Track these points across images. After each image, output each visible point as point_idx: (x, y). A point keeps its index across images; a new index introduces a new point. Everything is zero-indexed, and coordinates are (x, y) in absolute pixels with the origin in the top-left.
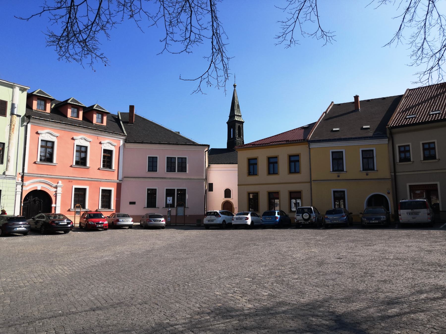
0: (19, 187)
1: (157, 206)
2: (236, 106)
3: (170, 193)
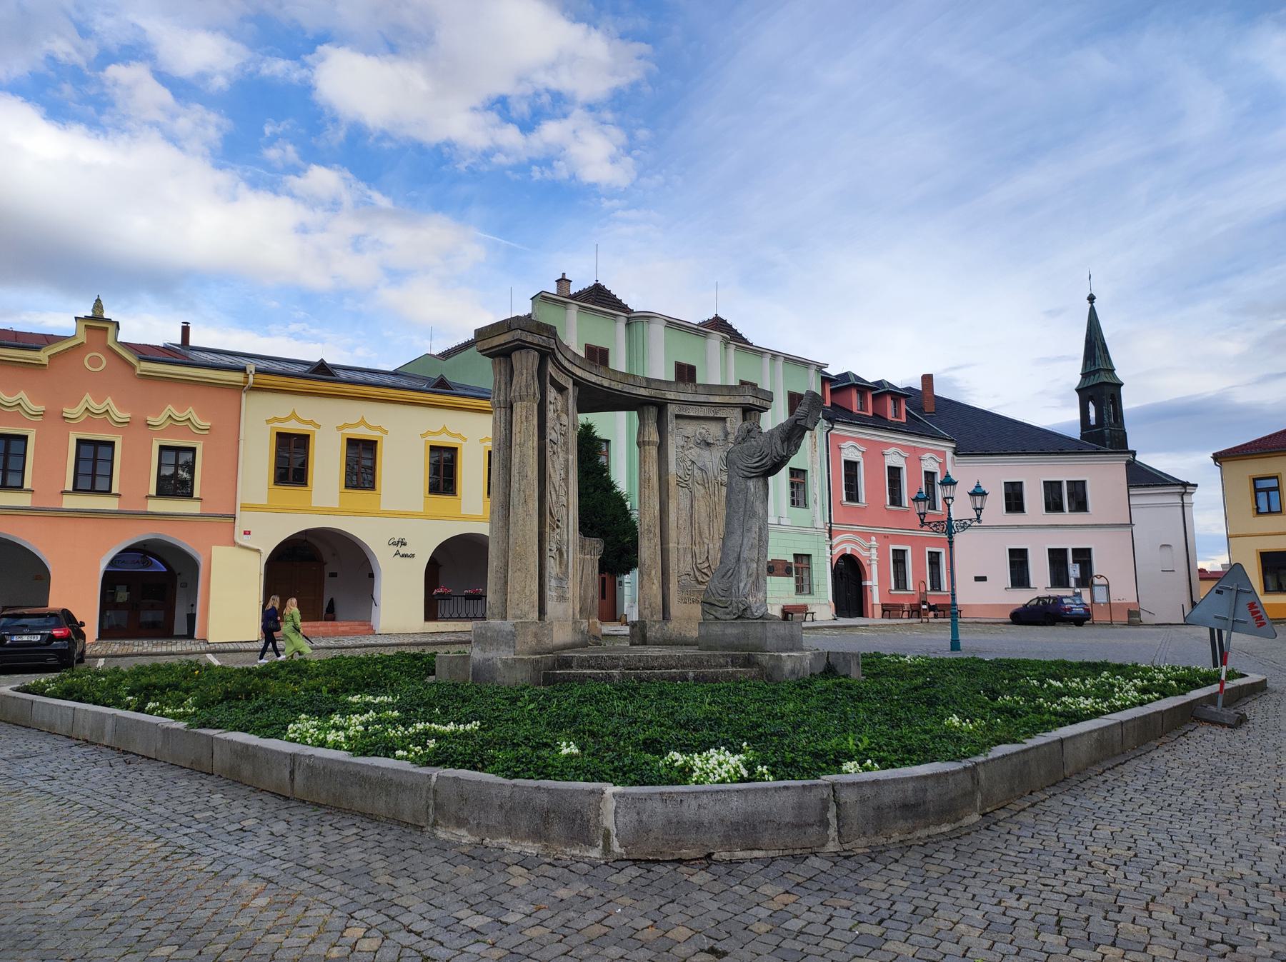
0: (828, 548)
1: (1032, 585)
2: (1101, 348)
3: (1057, 558)
